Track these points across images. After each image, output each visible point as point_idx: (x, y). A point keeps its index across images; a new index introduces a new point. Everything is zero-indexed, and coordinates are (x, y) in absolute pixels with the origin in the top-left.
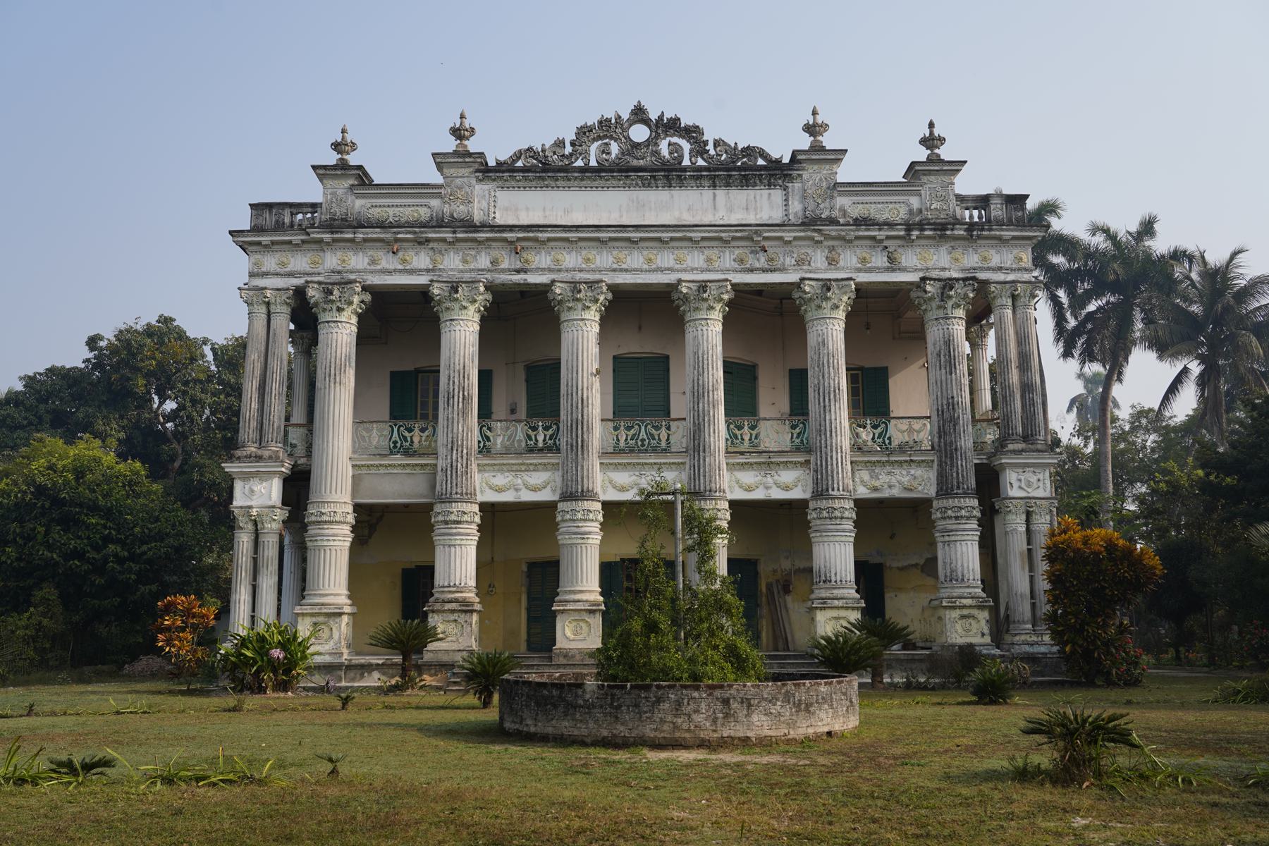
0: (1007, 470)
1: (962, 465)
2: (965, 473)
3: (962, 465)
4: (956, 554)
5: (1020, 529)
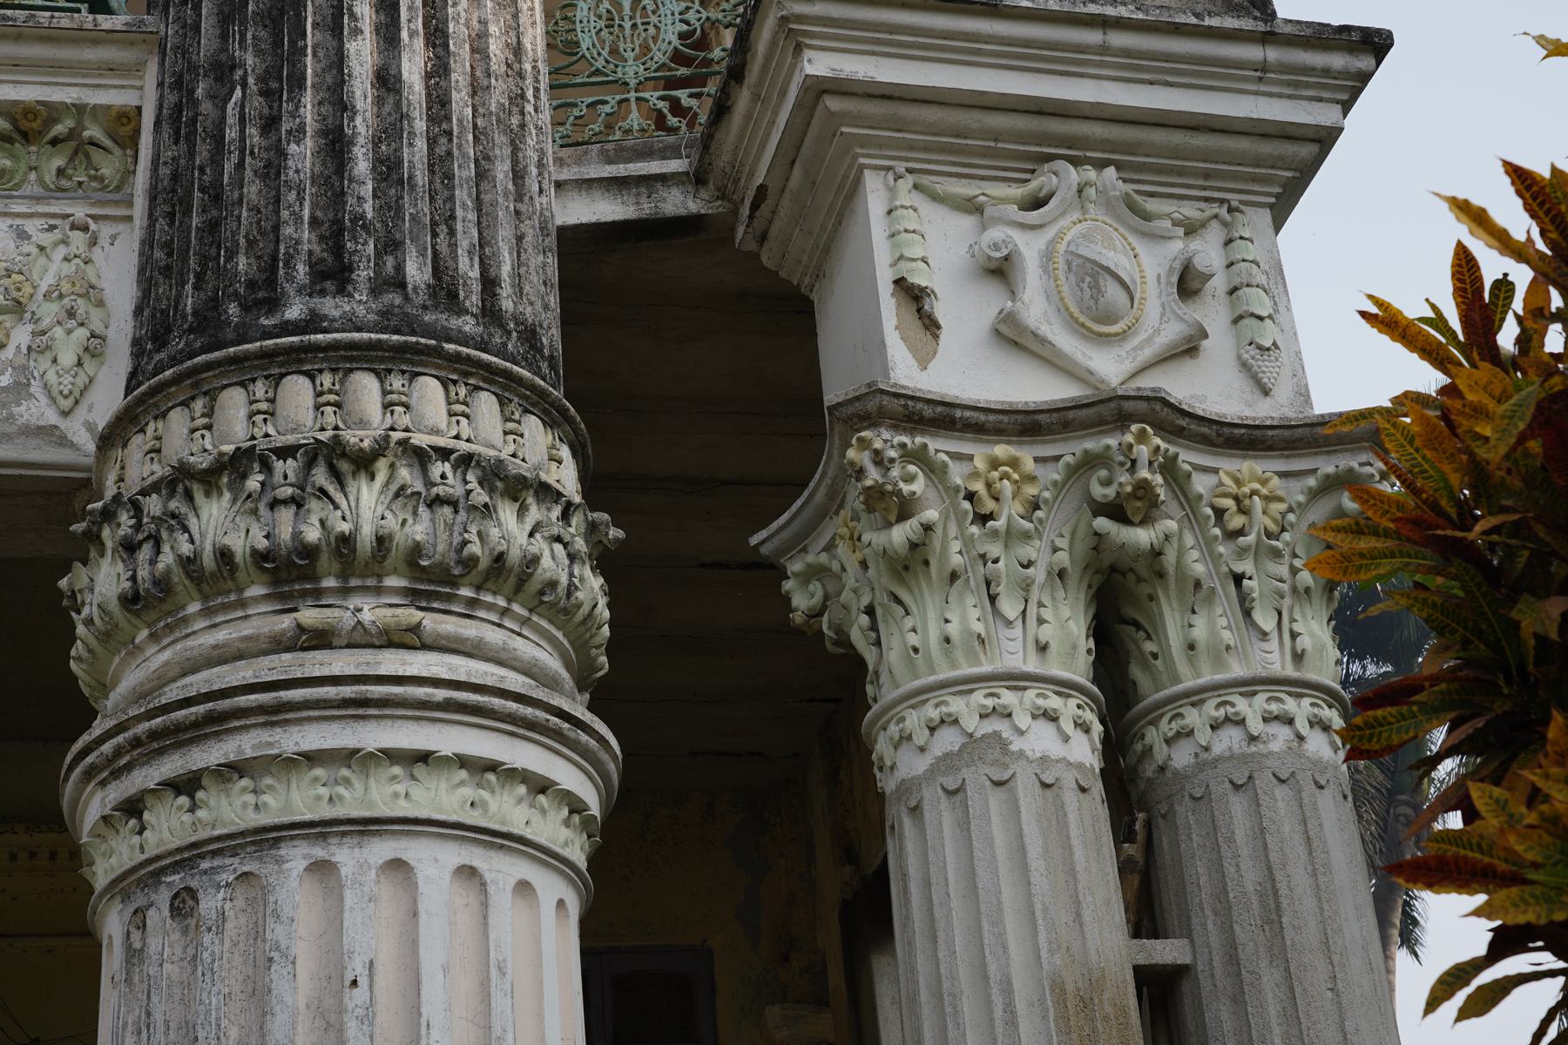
0: (875, 194)
1: (387, 81)
2: (416, 154)
3: (387, 81)
4: (259, 996)
5: (1040, 741)
